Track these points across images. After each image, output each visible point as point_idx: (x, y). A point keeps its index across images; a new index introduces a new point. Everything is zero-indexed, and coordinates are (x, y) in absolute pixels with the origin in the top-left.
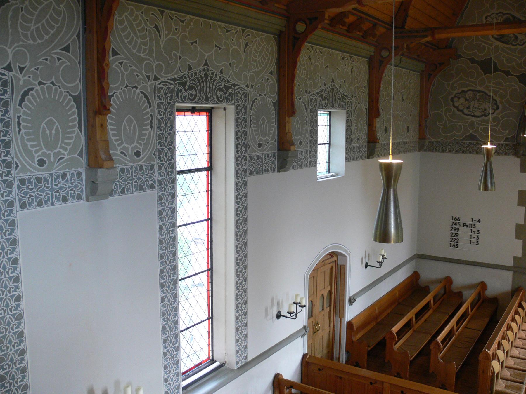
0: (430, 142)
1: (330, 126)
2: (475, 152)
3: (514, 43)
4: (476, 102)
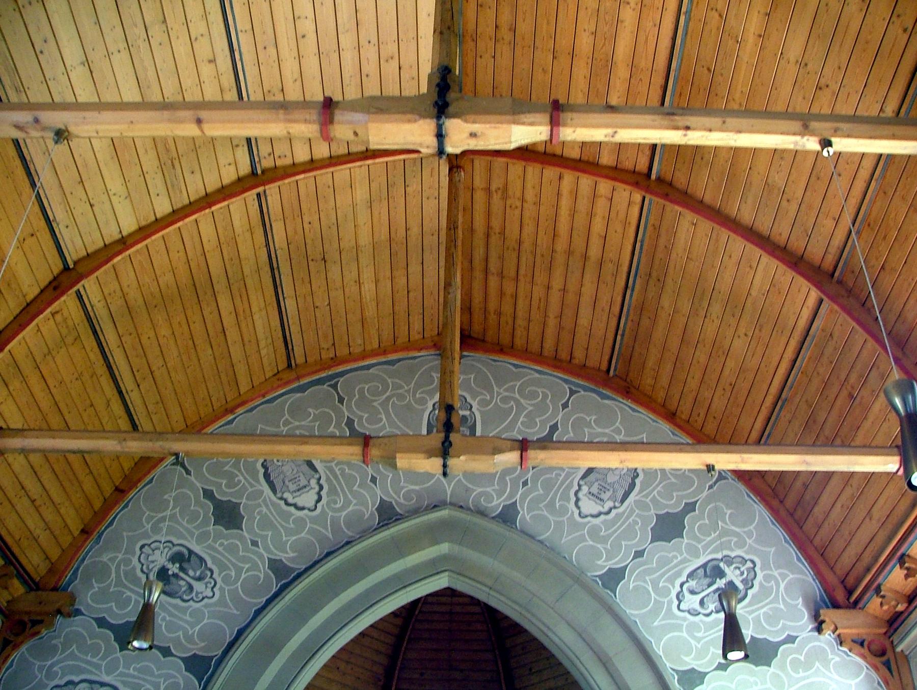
3: (185, 597)
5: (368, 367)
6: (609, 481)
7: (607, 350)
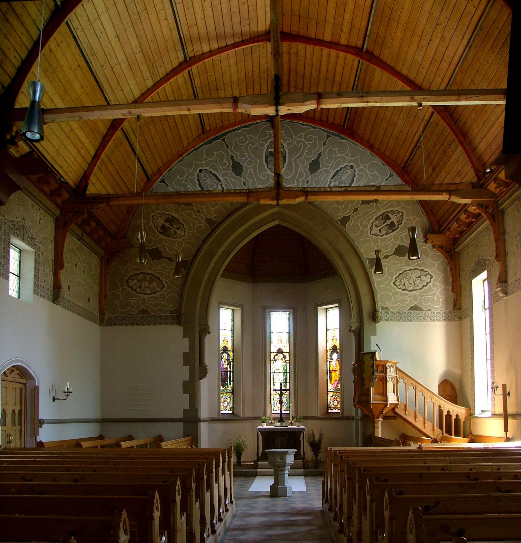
0: (109, 317)
1: (20, 261)
2: (147, 324)
4: (147, 283)
5: (237, 130)
6: (343, 179)
7: (343, 118)
